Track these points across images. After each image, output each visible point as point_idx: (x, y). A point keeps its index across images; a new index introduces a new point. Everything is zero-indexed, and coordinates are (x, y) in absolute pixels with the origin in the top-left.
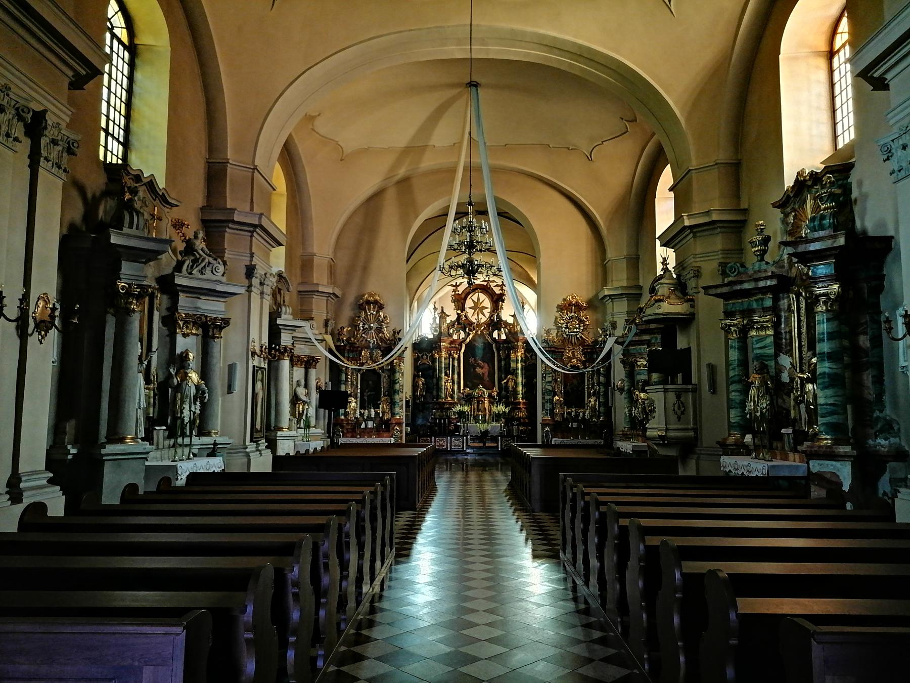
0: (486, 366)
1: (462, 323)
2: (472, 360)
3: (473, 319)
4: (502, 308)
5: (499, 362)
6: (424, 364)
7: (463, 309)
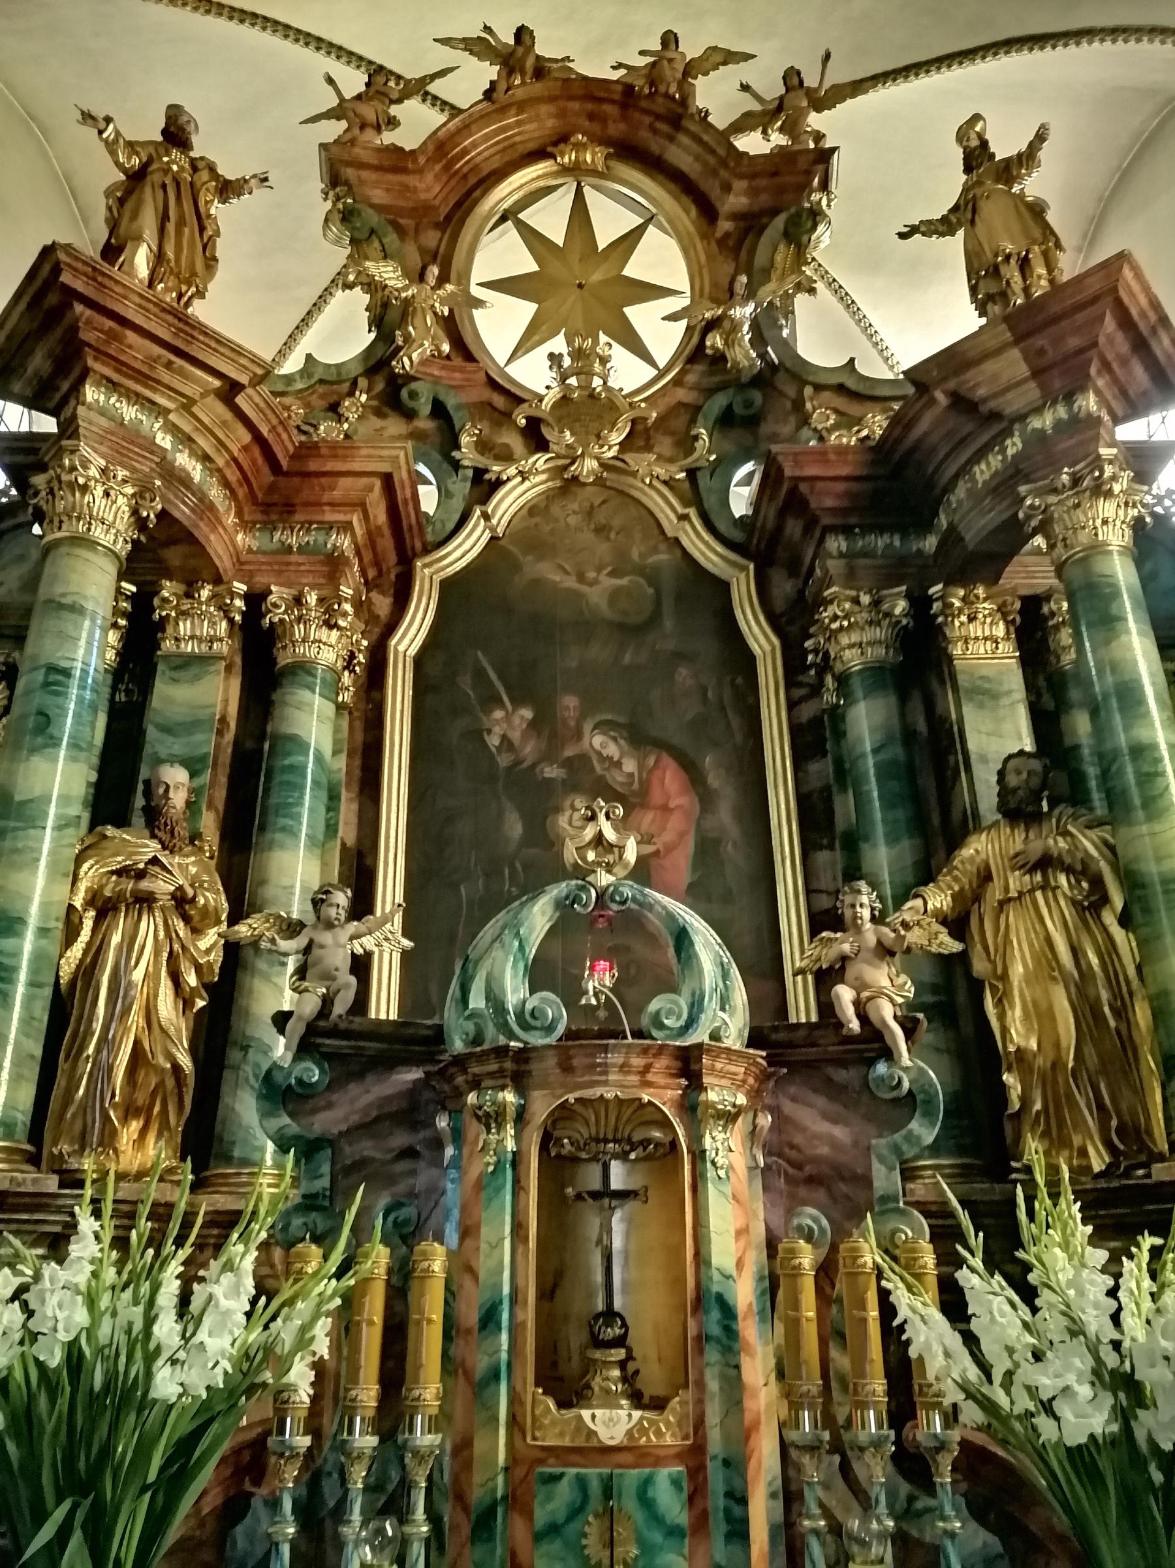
0: (670, 781)
2: (508, 725)
3: (534, 374)
5: (815, 738)
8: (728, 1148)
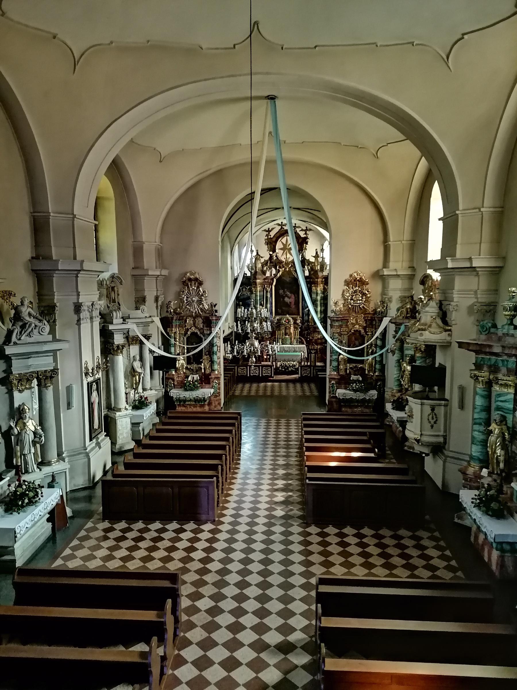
0: (293, 296)
1: (274, 262)
2: (281, 291)
3: (283, 259)
4: (306, 249)
6: (244, 295)
7: (274, 251)
8: (292, 328)
